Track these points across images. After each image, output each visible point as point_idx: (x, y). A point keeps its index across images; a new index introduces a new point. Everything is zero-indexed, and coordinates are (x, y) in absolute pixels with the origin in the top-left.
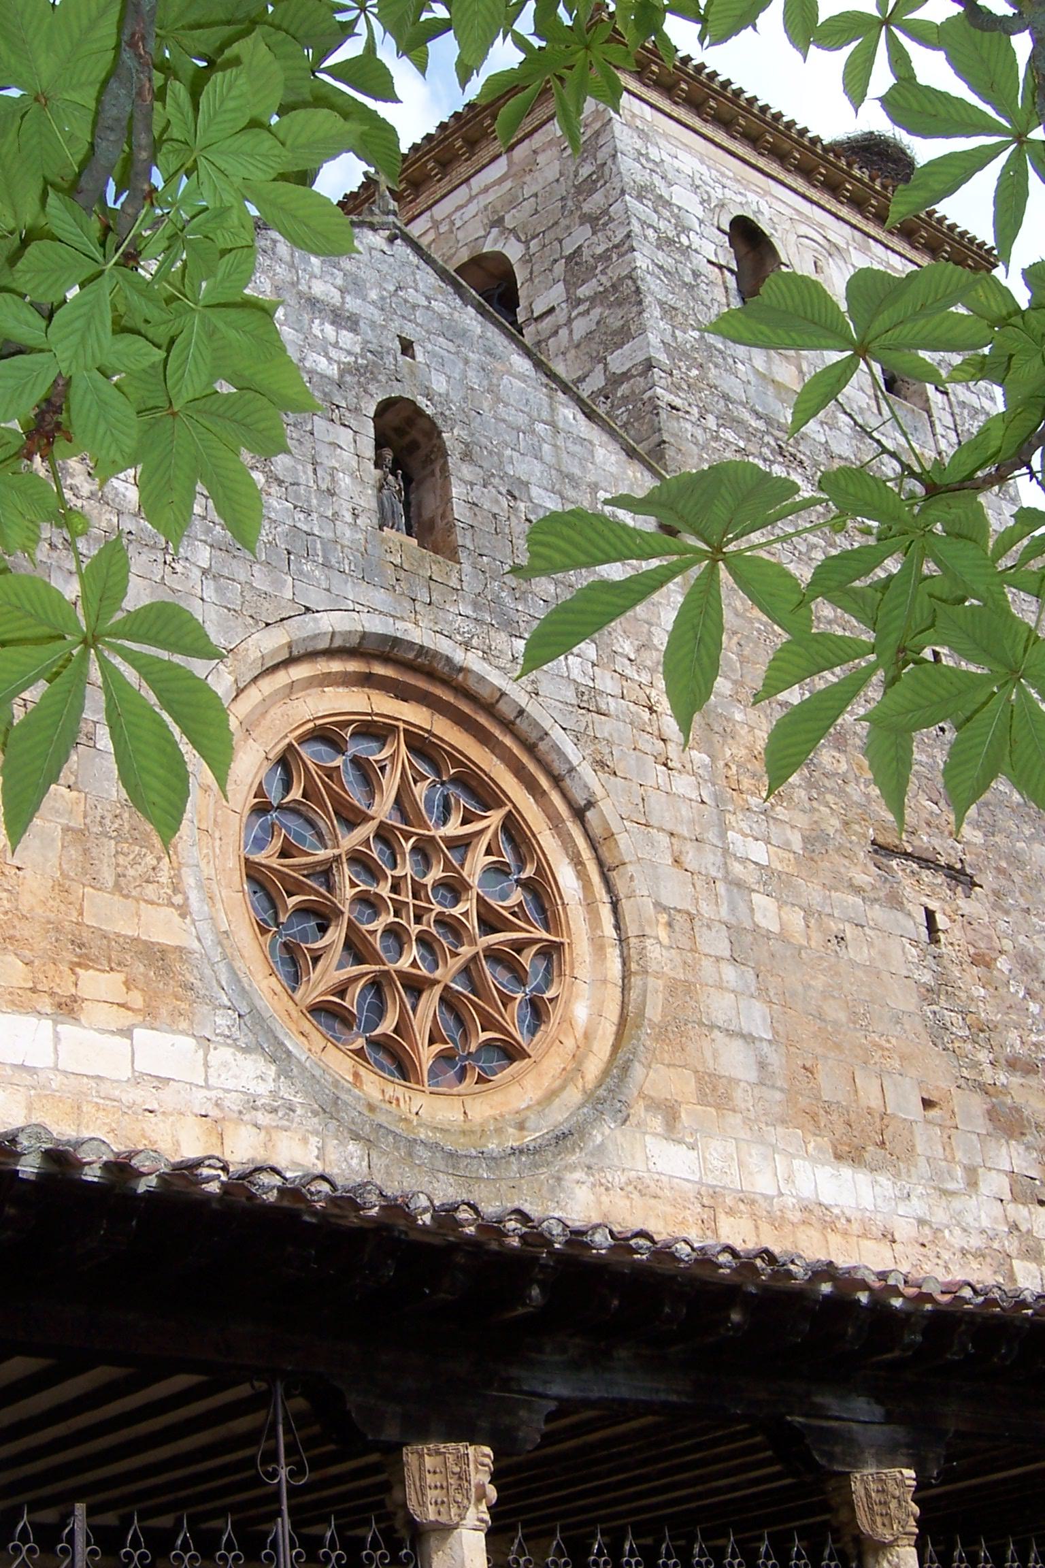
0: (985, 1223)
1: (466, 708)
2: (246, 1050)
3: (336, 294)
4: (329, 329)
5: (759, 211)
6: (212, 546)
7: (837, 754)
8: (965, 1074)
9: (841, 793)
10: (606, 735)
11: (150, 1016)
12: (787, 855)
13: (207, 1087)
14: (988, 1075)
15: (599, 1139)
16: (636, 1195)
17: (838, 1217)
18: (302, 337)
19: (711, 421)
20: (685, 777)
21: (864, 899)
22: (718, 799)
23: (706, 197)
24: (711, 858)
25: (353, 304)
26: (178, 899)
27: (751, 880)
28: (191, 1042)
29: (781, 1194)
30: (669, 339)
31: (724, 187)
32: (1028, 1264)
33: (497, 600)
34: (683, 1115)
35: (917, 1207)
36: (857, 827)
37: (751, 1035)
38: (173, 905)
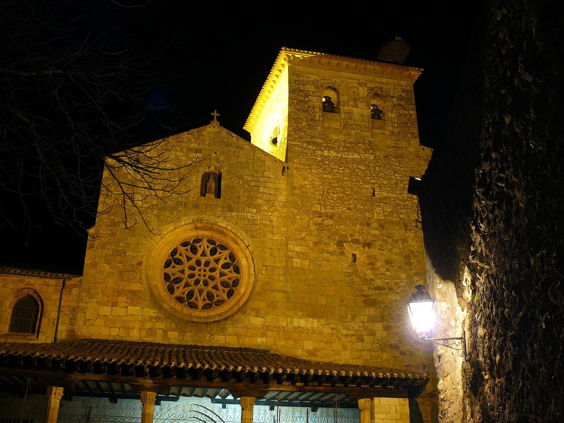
0: (356, 328)
1: (221, 229)
2: (150, 308)
4: (194, 154)
6: (157, 210)
7: (329, 220)
8: (357, 293)
9: (328, 231)
10: (255, 229)
11: (132, 304)
12: (307, 248)
13: (142, 315)
14: (366, 293)
15: (237, 318)
16: (245, 329)
17: (305, 330)
18: (186, 158)
19: (305, 145)
22: (288, 238)
23: (317, 85)
25: (200, 147)
26: (140, 281)
28: (139, 308)
29: (287, 326)
30: (295, 127)
31: (324, 80)
33: (230, 205)
34: (261, 311)
35: (332, 326)
36: (333, 237)
37: (286, 291)
38: (139, 282)
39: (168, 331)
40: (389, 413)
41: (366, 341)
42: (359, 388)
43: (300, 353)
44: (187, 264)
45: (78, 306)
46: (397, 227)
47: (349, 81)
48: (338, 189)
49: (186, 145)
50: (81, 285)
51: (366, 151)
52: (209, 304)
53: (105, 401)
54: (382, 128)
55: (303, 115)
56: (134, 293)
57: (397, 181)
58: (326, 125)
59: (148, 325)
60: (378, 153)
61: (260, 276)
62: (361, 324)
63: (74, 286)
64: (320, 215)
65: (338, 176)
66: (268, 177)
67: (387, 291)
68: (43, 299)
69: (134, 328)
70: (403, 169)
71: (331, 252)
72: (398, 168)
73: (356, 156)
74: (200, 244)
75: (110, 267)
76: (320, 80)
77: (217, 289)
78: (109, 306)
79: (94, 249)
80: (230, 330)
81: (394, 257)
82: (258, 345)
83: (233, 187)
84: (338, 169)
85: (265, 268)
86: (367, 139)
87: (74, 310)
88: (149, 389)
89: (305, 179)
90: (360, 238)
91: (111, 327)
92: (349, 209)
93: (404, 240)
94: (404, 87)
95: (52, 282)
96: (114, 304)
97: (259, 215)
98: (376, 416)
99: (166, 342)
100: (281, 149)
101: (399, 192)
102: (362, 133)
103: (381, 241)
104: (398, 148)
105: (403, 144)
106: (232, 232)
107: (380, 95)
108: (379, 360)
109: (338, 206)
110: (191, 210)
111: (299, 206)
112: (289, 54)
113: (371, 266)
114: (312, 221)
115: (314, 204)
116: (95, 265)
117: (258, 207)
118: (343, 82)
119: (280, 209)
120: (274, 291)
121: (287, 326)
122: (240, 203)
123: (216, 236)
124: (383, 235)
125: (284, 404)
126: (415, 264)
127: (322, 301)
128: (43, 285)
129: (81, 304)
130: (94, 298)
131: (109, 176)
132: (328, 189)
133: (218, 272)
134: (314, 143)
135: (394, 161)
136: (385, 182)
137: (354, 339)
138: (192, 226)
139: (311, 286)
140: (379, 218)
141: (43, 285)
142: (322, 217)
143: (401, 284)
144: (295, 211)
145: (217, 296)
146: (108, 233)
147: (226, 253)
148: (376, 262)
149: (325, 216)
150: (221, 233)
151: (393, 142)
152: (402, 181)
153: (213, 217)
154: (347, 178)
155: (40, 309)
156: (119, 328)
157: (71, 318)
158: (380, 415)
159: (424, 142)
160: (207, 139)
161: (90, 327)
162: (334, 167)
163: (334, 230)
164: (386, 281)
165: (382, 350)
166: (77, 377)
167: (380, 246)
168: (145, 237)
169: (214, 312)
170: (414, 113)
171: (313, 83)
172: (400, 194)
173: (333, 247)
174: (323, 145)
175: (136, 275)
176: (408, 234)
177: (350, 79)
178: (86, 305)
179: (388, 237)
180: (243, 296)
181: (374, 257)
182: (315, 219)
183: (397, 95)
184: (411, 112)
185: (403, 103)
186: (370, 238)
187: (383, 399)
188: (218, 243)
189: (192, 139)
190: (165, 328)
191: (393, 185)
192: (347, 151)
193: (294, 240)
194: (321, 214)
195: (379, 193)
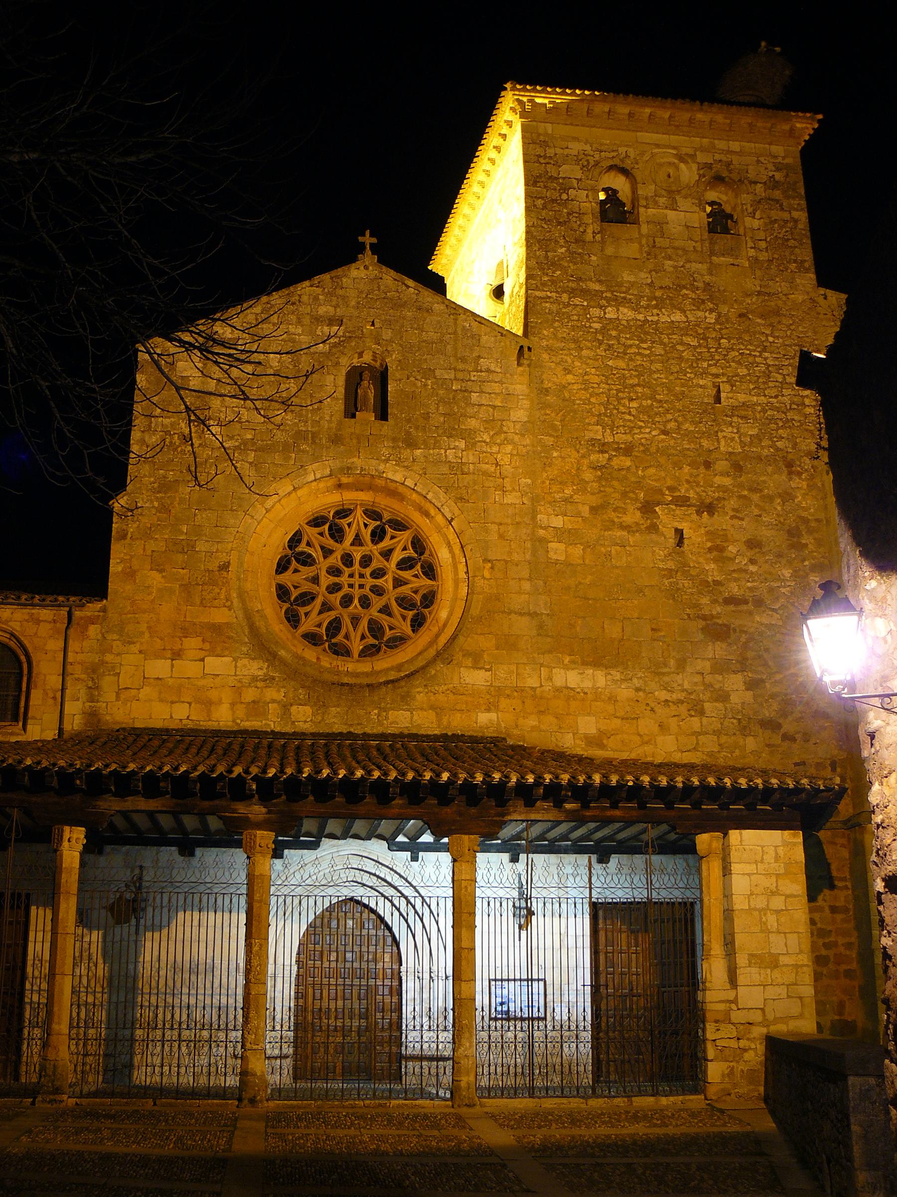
2: (253, 659)
3: (331, 309)
5: (627, 156)
6: (255, 451)
7: (623, 458)
11: (213, 653)
13: (236, 675)
15: (433, 672)
16: (451, 696)
17: (578, 693)
19: (565, 297)
20: (514, 493)
21: (628, 532)
22: (535, 500)
24: (524, 531)
25: (339, 312)
26: (228, 604)
27: (549, 537)
29: (541, 686)
30: (542, 259)
31: (601, 151)
32: (717, 704)
33: (408, 433)
34: (485, 656)
36: (631, 495)
39: (291, 705)
40: (762, 861)
41: (708, 713)
42: (697, 812)
43: (569, 743)
44: (323, 564)
45: (103, 663)
46: (770, 469)
47: (656, 150)
48: (639, 389)
49: (308, 310)
50: (105, 619)
51: (698, 304)
52: (373, 646)
53: (170, 853)
54: (731, 252)
55: (557, 232)
56: (216, 629)
57: (767, 368)
58: (610, 251)
59: (250, 695)
60: (724, 309)
61: (479, 583)
62: (698, 678)
63: (92, 621)
64: (603, 448)
65: (639, 363)
66: (488, 371)
67: (750, 606)
68: (30, 649)
69: (220, 702)
70: (781, 340)
71: (630, 526)
72: (771, 339)
73: (678, 317)
74: (349, 519)
75: (163, 577)
76: (592, 153)
77: (390, 615)
78: (166, 659)
79: (128, 540)
80: (420, 697)
81: (766, 533)
82: (481, 727)
83: (413, 396)
84: (638, 347)
85: (490, 565)
86: (699, 277)
87: (94, 671)
88: (259, 826)
89: (567, 371)
90: (692, 494)
91: (172, 702)
92: (665, 432)
93: (787, 496)
94: (780, 160)
95: (46, 614)
96: (177, 655)
97: (471, 453)
98: (735, 868)
99: (289, 729)
100: (514, 309)
101: (773, 392)
102: (688, 266)
103: (735, 499)
104: (769, 294)
105: (779, 286)
106: (417, 492)
107: (727, 179)
108: (737, 752)
109: (641, 427)
110: (327, 448)
111: (556, 431)
112: (521, 98)
113: (715, 553)
114: (586, 461)
115: (589, 424)
116: (130, 574)
117: (469, 436)
118: (642, 154)
119: (517, 438)
120: (509, 614)
121: (541, 686)
122: (430, 430)
123: (383, 502)
124: (741, 486)
125: (539, 849)
126: (810, 546)
127: (614, 631)
128: (27, 621)
129: (109, 658)
130: (134, 643)
131: (148, 386)
132: (618, 391)
133: (389, 577)
134: (584, 293)
135: (759, 325)
136: (743, 371)
137: (683, 709)
138: (331, 482)
139: (589, 599)
140: (730, 450)
141: (27, 621)
142: (606, 452)
143: (783, 590)
144: (549, 441)
145: (391, 628)
146: (154, 507)
147: (405, 537)
148: (725, 544)
149: (615, 450)
150: (393, 493)
151: (757, 282)
152: (779, 368)
153: (374, 462)
154: (659, 366)
155: (25, 671)
156: (190, 704)
157: (90, 688)
158: (742, 866)
159: (824, 281)
160: (352, 293)
161: (129, 705)
162: (630, 342)
163: (633, 479)
164: (749, 584)
165: (744, 730)
166: (110, 805)
167: (733, 510)
168: (232, 510)
169: (385, 663)
170: (802, 216)
171: (578, 161)
172: (776, 397)
173: (633, 516)
174: (604, 295)
175: (217, 590)
176: (795, 482)
177: (658, 146)
178: (118, 660)
179: (751, 490)
180: (445, 625)
181: (721, 533)
182: (594, 457)
183: (765, 178)
184: (795, 214)
185: (777, 194)
186: (712, 494)
187: (748, 834)
188: (386, 516)
189: (321, 297)
190: (285, 699)
191: (759, 377)
192: (656, 306)
193: (550, 503)
194: (604, 444)
195: (730, 395)
